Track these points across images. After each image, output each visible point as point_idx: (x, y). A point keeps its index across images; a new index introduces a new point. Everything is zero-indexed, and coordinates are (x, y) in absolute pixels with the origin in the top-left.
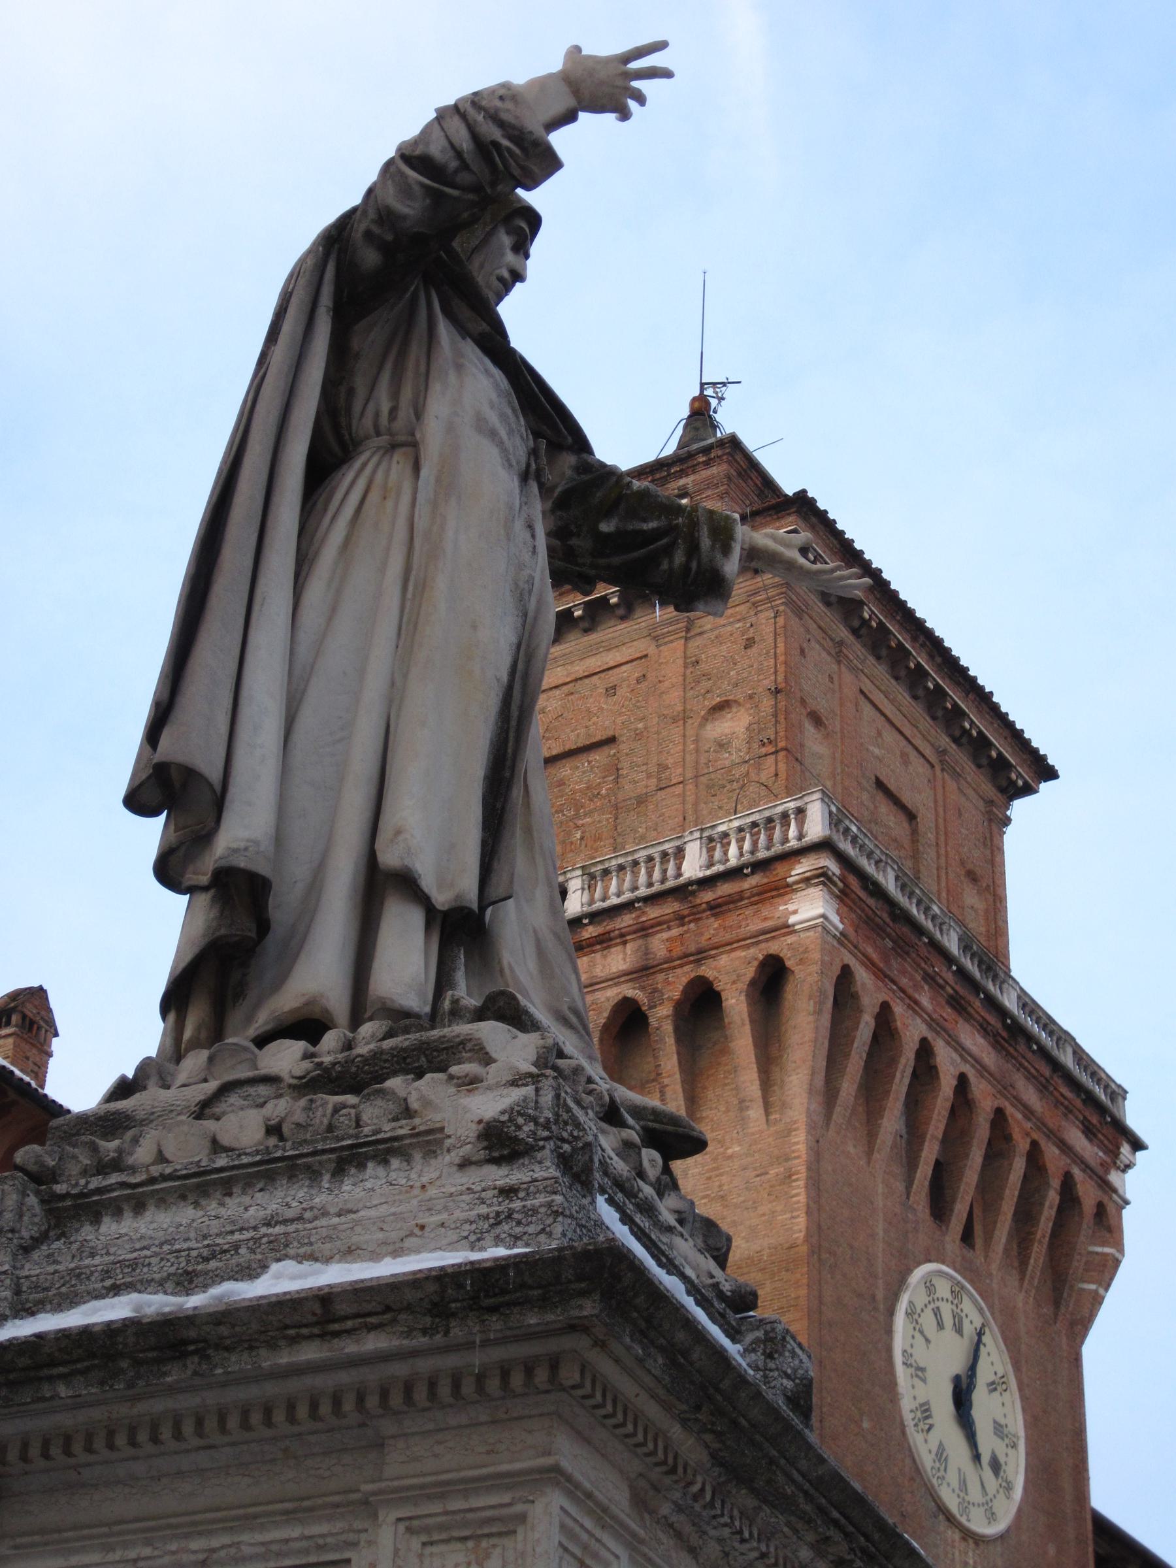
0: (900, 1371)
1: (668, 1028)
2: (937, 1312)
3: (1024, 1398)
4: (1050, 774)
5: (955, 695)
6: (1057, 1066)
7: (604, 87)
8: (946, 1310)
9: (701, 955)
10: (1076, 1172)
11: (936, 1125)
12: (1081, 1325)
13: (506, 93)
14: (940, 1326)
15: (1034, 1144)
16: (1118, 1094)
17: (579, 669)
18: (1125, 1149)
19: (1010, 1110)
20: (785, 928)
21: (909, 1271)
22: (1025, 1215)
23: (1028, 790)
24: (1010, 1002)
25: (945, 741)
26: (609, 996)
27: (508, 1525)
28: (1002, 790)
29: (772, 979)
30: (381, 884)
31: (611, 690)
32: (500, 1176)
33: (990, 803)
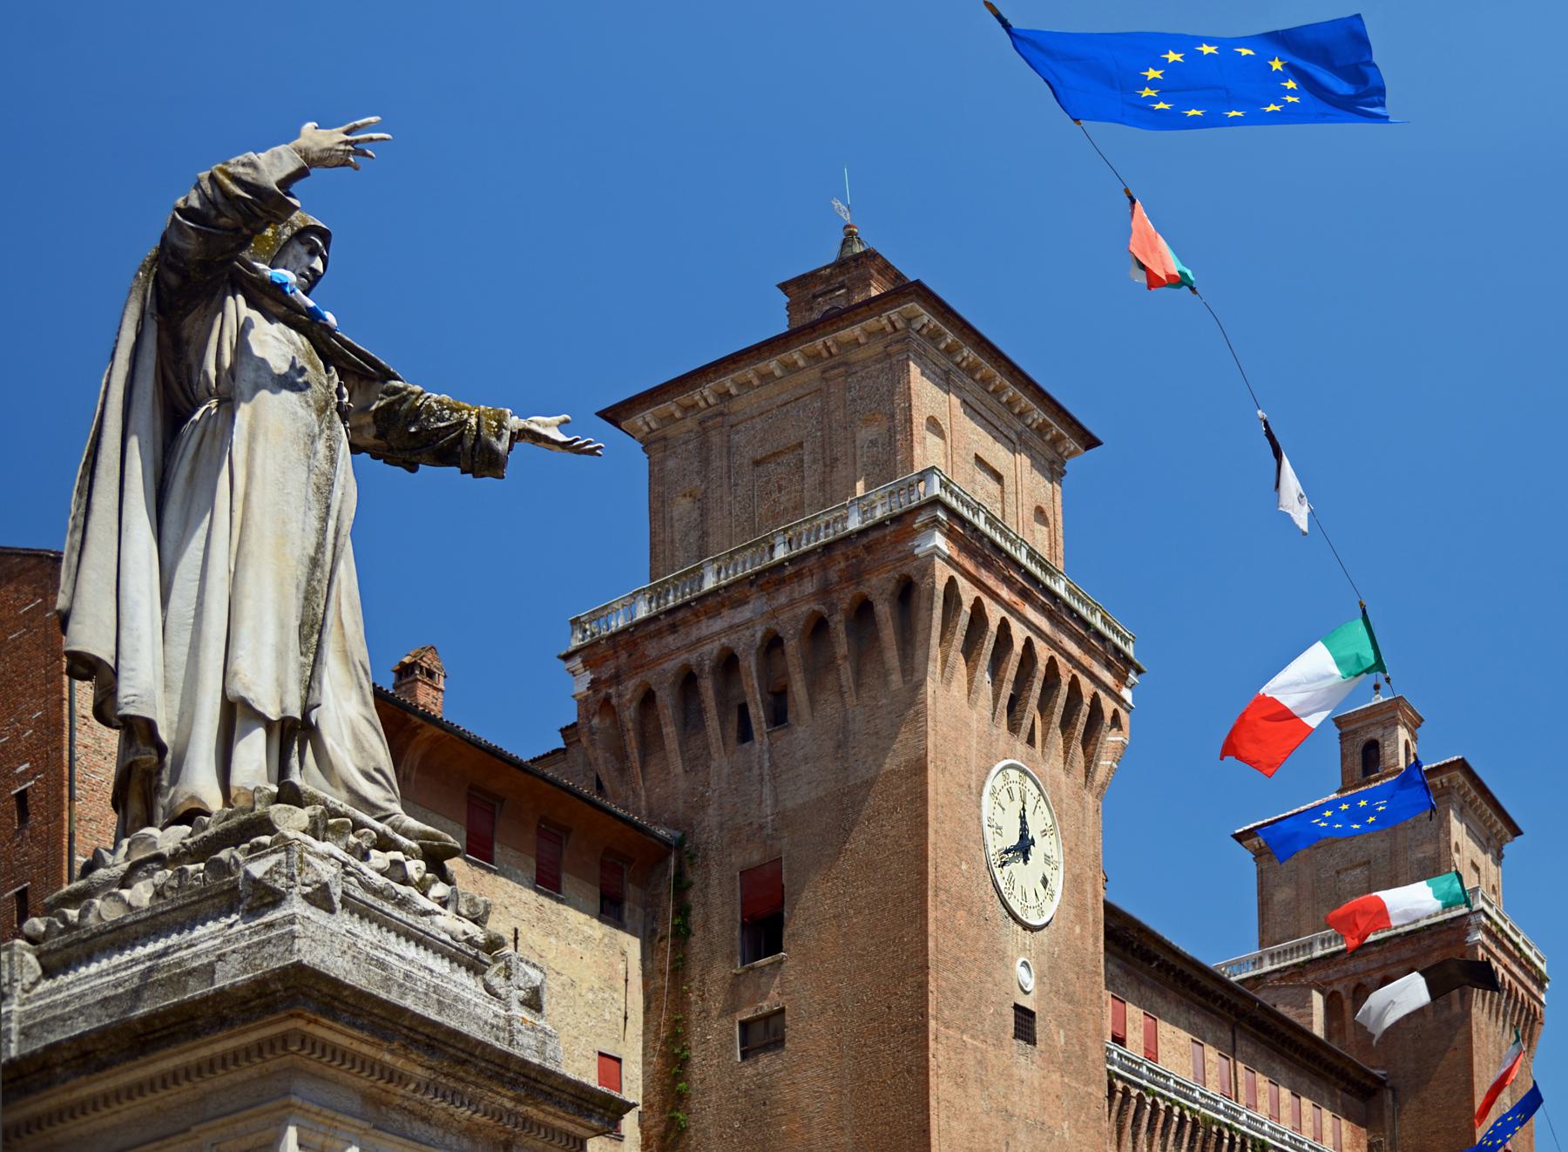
0: (987, 830)
1: (841, 627)
2: (1009, 791)
8: (1016, 788)
14: (1012, 799)
15: (1074, 677)
26: (804, 609)
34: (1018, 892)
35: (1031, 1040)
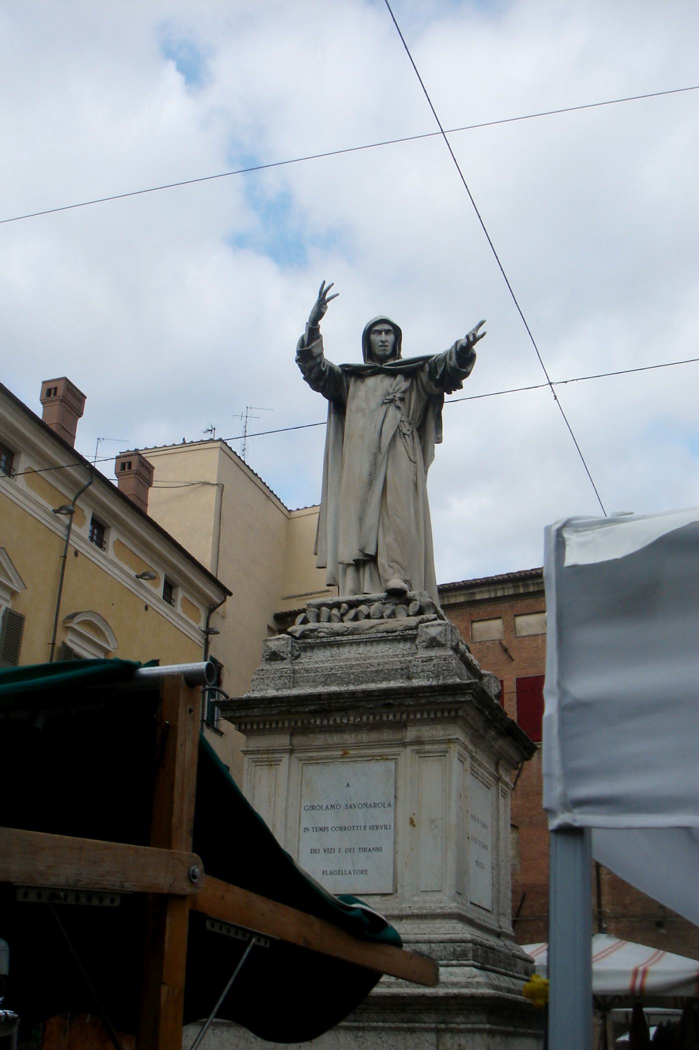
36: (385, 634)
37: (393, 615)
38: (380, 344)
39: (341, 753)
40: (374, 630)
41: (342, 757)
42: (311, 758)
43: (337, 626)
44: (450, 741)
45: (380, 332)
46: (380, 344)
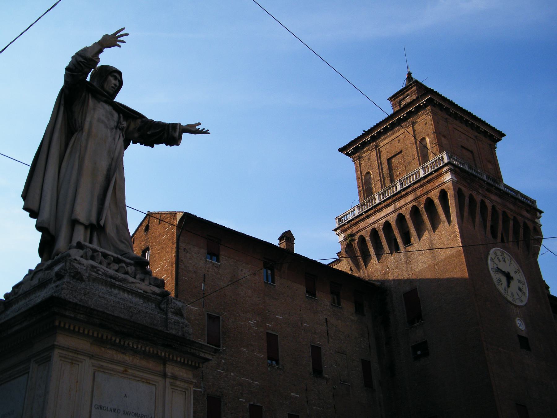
2: (498, 258)
3: (524, 273)
4: (504, 135)
5: (476, 123)
6: (516, 199)
7: (111, 41)
9: (428, 192)
10: (526, 221)
11: (489, 218)
12: (536, 254)
13: (86, 50)
14: (500, 261)
16: (534, 202)
17: (391, 138)
18: (538, 214)
19: (506, 210)
20: (444, 183)
21: (489, 251)
22: (516, 233)
23: (499, 140)
24: (502, 187)
25: (477, 134)
27: (48, 359)
28: (493, 141)
29: (443, 195)
30: (74, 223)
31: (399, 141)
32: (58, 283)
33: (490, 145)
34: (510, 294)
35: (528, 348)
36: (142, 292)
37: (143, 280)
38: (113, 85)
39: (122, 369)
40: (133, 285)
41: (122, 373)
42: (102, 367)
43: (111, 272)
44: (191, 383)
45: (116, 78)
46: (113, 85)
